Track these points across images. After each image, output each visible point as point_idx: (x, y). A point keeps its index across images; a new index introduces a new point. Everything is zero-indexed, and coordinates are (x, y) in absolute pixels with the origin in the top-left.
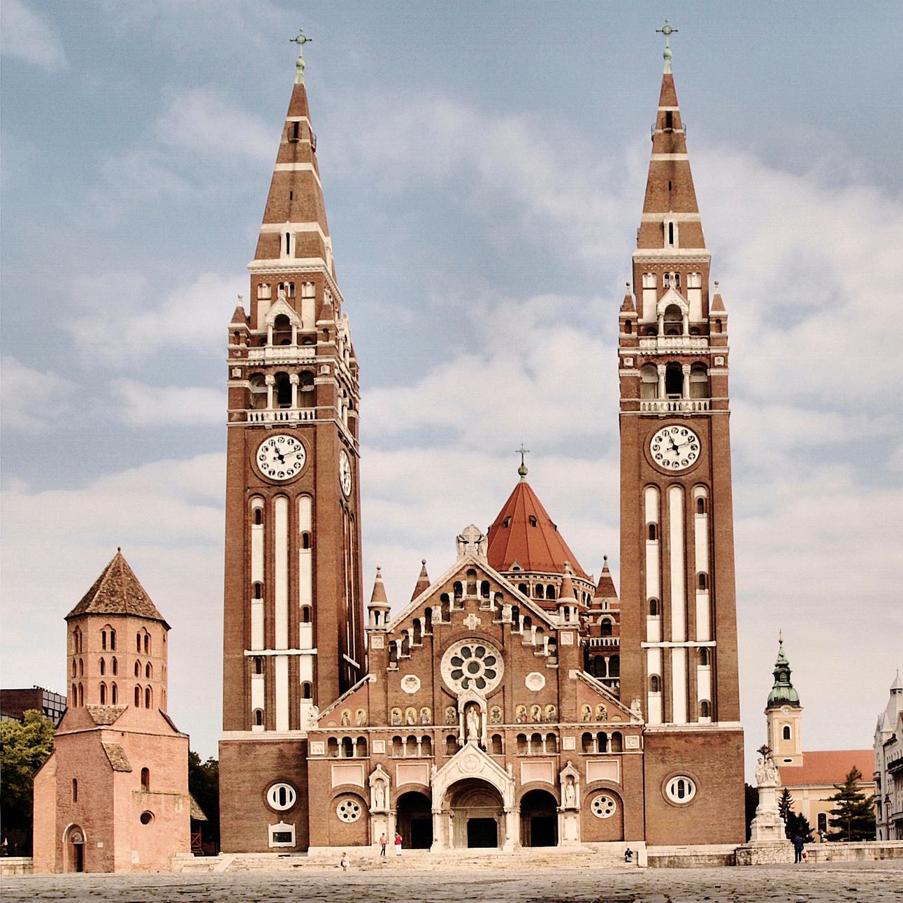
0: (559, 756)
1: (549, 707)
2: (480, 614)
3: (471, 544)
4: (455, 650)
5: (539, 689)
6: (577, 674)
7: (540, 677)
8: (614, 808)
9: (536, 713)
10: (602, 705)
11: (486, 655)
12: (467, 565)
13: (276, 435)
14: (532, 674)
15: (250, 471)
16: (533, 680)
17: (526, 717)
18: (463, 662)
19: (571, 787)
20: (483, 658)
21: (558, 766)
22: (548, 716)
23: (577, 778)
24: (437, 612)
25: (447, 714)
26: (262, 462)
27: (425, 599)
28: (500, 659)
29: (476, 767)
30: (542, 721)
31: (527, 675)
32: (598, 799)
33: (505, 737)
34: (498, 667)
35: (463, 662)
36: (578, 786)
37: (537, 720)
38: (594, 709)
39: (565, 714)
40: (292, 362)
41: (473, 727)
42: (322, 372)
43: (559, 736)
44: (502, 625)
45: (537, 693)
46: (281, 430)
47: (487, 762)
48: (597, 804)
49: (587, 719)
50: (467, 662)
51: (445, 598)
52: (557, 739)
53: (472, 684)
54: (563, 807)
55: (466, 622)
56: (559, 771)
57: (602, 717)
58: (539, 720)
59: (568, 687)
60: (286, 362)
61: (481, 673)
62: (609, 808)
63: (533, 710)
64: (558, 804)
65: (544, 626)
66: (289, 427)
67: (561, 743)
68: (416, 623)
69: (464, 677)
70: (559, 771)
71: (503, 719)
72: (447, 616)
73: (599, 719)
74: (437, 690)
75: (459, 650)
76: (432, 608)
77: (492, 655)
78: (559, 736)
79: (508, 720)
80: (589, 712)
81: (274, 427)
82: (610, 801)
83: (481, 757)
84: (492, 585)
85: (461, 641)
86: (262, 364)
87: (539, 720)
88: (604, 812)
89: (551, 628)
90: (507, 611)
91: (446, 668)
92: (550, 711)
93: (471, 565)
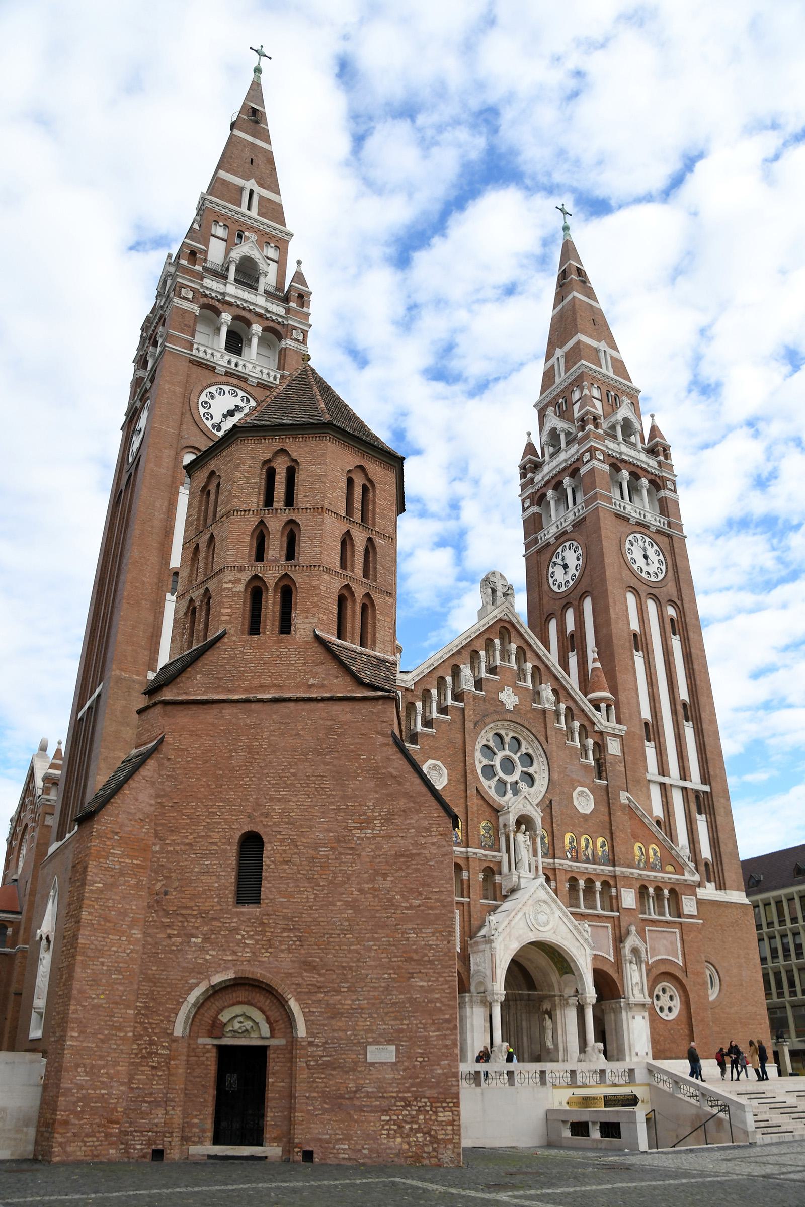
0: (619, 917)
1: (600, 840)
2: (517, 689)
3: (499, 594)
4: (486, 737)
5: (588, 812)
6: (628, 798)
7: (587, 795)
8: (677, 1004)
9: (587, 847)
10: (654, 846)
11: (523, 750)
12: (500, 620)
13: (227, 384)
14: (579, 789)
15: (188, 415)
16: (580, 798)
17: (577, 851)
18: (495, 754)
19: (634, 967)
20: (519, 754)
21: (617, 932)
22: (600, 854)
23: (643, 955)
24: (466, 671)
25: (482, 832)
26: (206, 411)
27: (455, 650)
28: (542, 759)
29: (548, 923)
30: (594, 863)
31: (574, 790)
32: (657, 990)
33: (556, 880)
34: (539, 769)
35: (495, 754)
36: (644, 966)
37: (588, 858)
38: (647, 851)
39: (619, 856)
40: (257, 310)
41: (525, 855)
42: (295, 336)
43: (616, 887)
44: (544, 711)
45: (585, 816)
46: (236, 382)
47: (561, 915)
48: (658, 997)
49: (642, 865)
50: (500, 755)
51: (475, 655)
52: (614, 890)
53: (522, 785)
54: (632, 1000)
55: (502, 696)
56: (619, 940)
57: (656, 864)
58: (591, 858)
59: (618, 815)
60: (251, 307)
61: (516, 776)
62: (672, 1004)
63: (583, 843)
64: (621, 993)
65: (586, 723)
66: (245, 380)
67: (618, 897)
68: (441, 680)
69: (497, 778)
70: (619, 940)
71: (551, 852)
72: (479, 684)
73: (653, 868)
74: (472, 791)
75: (490, 735)
76: (462, 666)
77: (530, 751)
78: (616, 887)
79: (558, 853)
80: (643, 854)
81: (227, 374)
82: (672, 993)
83: (553, 905)
84: (529, 655)
85: (497, 723)
86: (220, 297)
87: (591, 858)
88: (666, 1011)
89: (596, 728)
90: (547, 692)
91: (479, 761)
92: (602, 847)
93: (505, 621)
